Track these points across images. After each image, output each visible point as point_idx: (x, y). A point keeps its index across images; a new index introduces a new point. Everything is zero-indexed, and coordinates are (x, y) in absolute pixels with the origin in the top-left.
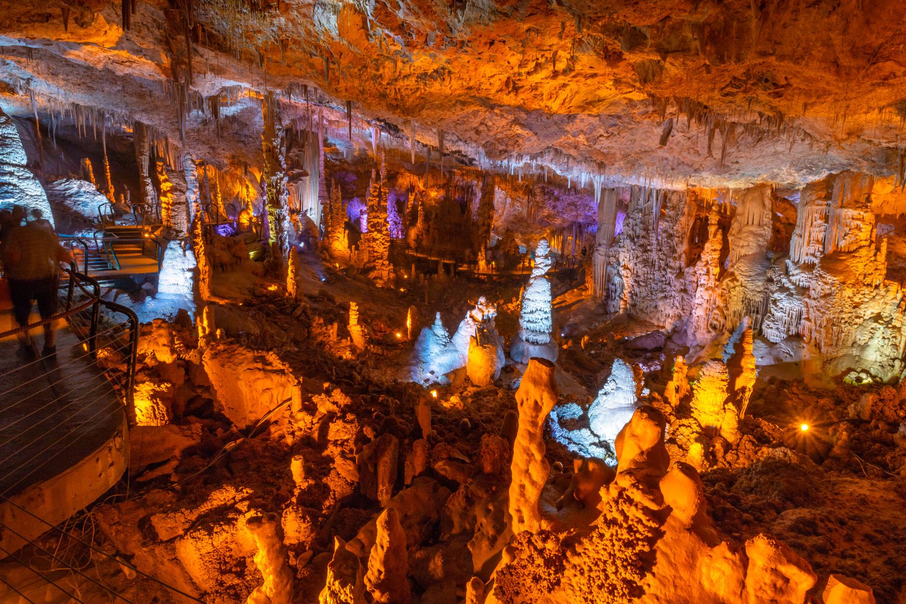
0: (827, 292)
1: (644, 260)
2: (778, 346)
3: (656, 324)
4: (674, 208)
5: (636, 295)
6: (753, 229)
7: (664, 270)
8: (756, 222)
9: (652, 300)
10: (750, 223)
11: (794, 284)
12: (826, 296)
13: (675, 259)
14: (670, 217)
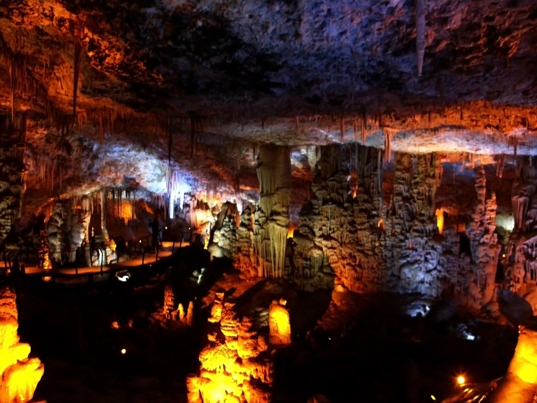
3: (401, 292)
4: (408, 170)
5: (360, 266)
7: (402, 234)
9: (387, 269)
13: (423, 222)
14: (404, 179)
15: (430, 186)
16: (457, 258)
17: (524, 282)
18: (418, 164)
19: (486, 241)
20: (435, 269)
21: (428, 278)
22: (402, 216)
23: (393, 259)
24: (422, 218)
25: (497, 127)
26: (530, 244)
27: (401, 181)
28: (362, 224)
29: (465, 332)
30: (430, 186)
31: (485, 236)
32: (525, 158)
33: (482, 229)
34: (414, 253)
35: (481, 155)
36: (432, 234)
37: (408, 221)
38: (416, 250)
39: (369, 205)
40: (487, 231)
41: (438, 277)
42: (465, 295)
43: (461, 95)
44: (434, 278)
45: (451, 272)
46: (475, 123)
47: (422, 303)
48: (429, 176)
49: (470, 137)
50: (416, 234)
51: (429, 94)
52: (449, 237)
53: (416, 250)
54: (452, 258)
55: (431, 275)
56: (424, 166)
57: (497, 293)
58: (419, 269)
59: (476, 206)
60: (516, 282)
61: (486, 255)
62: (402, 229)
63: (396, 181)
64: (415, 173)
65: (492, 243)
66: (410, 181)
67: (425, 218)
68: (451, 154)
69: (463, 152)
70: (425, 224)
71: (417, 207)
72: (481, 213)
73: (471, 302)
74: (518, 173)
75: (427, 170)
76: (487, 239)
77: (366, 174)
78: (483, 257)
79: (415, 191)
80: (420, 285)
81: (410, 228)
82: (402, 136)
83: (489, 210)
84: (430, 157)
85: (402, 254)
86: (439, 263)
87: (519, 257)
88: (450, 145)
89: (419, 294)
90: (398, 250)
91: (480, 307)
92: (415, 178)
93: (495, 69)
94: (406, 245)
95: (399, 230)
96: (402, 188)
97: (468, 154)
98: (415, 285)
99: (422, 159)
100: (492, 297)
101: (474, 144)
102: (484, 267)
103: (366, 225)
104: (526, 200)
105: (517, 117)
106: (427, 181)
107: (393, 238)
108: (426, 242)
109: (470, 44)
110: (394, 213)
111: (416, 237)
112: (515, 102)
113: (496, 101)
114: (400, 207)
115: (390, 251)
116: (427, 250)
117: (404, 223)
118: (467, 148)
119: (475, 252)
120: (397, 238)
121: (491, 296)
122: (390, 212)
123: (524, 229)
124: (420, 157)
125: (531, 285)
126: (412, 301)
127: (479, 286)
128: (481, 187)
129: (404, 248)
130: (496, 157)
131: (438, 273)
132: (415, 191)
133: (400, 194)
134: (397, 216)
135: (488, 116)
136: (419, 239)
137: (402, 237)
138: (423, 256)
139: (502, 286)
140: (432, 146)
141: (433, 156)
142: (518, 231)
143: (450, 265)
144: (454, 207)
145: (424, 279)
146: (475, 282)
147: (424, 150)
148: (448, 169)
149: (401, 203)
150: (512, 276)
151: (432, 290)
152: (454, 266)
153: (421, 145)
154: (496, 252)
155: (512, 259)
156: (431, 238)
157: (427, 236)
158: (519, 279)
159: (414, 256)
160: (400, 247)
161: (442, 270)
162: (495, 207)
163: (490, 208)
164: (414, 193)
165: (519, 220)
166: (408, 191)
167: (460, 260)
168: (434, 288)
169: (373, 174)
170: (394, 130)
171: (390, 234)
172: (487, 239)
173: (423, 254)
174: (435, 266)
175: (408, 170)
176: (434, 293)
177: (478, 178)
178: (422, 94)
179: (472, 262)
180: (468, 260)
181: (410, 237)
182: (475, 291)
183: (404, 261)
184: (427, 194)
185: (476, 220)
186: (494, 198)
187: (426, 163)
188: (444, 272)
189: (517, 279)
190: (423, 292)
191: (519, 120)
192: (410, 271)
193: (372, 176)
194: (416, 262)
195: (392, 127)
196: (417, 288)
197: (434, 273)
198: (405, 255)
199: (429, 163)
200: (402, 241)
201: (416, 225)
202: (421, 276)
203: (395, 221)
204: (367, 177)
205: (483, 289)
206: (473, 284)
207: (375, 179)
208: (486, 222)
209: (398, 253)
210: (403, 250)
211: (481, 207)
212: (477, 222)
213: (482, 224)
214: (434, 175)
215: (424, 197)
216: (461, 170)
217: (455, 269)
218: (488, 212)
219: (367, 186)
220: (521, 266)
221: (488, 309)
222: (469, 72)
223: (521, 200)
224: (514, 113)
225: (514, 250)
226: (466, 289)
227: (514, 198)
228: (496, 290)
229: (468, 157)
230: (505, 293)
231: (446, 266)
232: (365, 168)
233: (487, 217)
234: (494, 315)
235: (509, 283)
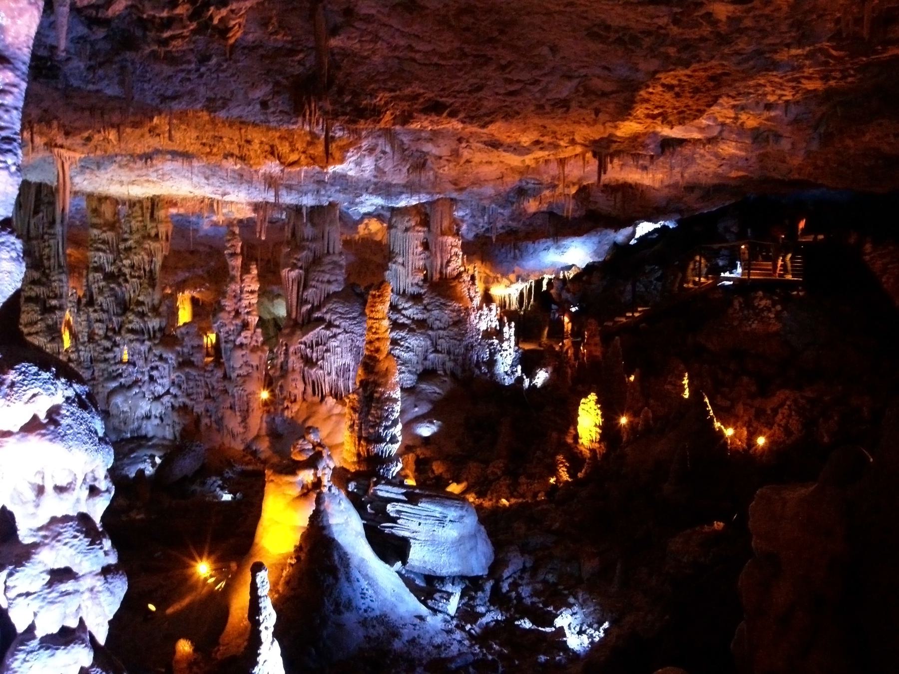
0: (456, 319)
1: (49, 327)
2: (418, 390)
4: (112, 226)
6: (335, 258)
7: (106, 337)
8: (336, 252)
10: (331, 251)
11: (409, 318)
12: (456, 323)
13: (142, 315)
14: (104, 242)
15: (151, 254)
16: (202, 373)
17: (304, 400)
18: (128, 216)
19: (245, 341)
20: (168, 392)
21: (157, 409)
22: (105, 306)
23: (95, 382)
24: (140, 309)
25: (242, 158)
26: (308, 342)
27: (100, 246)
28: (32, 323)
29: (218, 489)
30: (151, 254)
31: (243, 334)
32: (298, 209)
33: (238, 322)
34: (131, 369)
35: (232, 202)
36: (158, 335)
37: (117, 315)
38: (134, 365)
39: (42, 289)
40: (245, 326)
41: (173, 406)
42: (219, 430)
43: (164, 99)
44: (166, 408)
45: (194, 397)
46: (208, 150)
47: (149, 452)
48: (149, 237)
49: (208, 172)
50: (132, 337)
51: (109, 92)
52: (186, 339)
53: (134, 365)
54: (194, 372)
55: (162, 404)
56: (140, 219)
57: (266, 422)
58: (140, 395)
59: (227, 286)
60: (292, 402)
61: (246, 363)
62: (107, 329)
63: (91, 246)
64: (126, 232)
65: (254, 343)
66: (117, 246)
67: (145, 309)
68: (184, 199)
69: (204, 198)
70: (146, 319)
71: (130, 289)
72: (235, 297)
73: (227, 440)
74: (288, 233)
75: (146, 226)
76: (245, 337)
77: (33, 233)
78: (241, 367)
79: (127, 262)
80: (145, 422)
81: (120, 328)
82: (94, 167)
83: (248, 292)
84: (149, 204)
85: (110, 373)
86: (173, 383)
87: (295, 362)
88: (180, 184)
89: (145, 438)
90: (102, 366)
91: (242, 447)
92: (126, 240)
93: (214, 61)
94: (115, 357)
95: (101, 332)
96: (102, 258)
97: (212, 200)
98: (136, 424)
99: (137, 208)
100: (260, 429)
101: (218, 184)
102: (244, 382)
103: (40, 326)
104: (300, 274)
105: (261, 143)
106: (147, 246)
107: (91, 346)
108: (150, 349)
109: (163, 11)
110: (91, 302)
111: (131, 341)
112: (252, 119)
113: (222, 114)
114: (101, 291)
115: (88, 368)
116: (151, 362)
117: (110, 320)
118: (207, 191)
119: (229, 360)
120: (99, 345)
121: (258, 427)
122: (84, 301)
123: (300, 320)
124: (133, 203)
125: (313, 404)
126: (132, 451)
127: (238, 414)
128: (234, 255)
129: (112, 362)
130: (256, 207)
131: (172, 400)
132: (127, 262)
133: (99, 269)
134: (96, 307)
135: (221, 138)
136: (137, 345)
137: (108, 344)
138: (146, 373)
139: (272, 410)
140: (151, 185)
141: (154, 203)
142: (292, 323)
143: (191, 384)
144: (208, 289)
145: (150, 411)
146: (232, 408)
147: (139, 191)
148: (182, 226)
149: (102, 284)
150: (285, 393)
151: (165, 429)
152: (198, 386)
153: (133, 183)
154: (260, 358)
155: (285, 368)
156: (157, 342)
157: (150, 339)
158: (295, 396)
159: (130, 375)
160: (106, 360)
161: (179, 393)
162: (256, 286)
163: (249, 289)
164: (124, 266)
165: (291, 306)
166: (114, 263)
167: (206, 374)
168: (169, 425)
169: (46, 233)
170: (71, 154)
171: (86, 339)
172: (245, 337)
173: (146, 369)
174: (167, 389)
175: (112, 226)
176: (168, 433)
177: (229, 240)
178: (98, 91)
179: (226, 377)
180: (219, 374)
181: (122, 342)
182: (233, 422)
183: (114, 385)
184: (147, 269)
185: (227, 309)
186: (255, 272)
187: (143, 215)
188: (183, 397)
189: (293, 398)
190: (150, 435)
191: (267, 148)
192: (126, 401)
193: (46, 237)
194: (136, 383)
195: (69, 149)
196: (140, 427)
197: (166, 399)
198: (115, 374)
199: (148, 215)
200: (108, 350)
201: (130, 322)
202: (145, 407)
203: (94, 316)
204: (36, 238)
205: (244, 419)
206: (229, 412)
207: (52, 242)
208: (243, 311)
209: (104, 370)
210: (111, 365)
211: (235, 287)
212: (229, 312)
213: (237, 313)
214: (157, 235)
215: (142, 272)
216: (205, 226)
217: (199, 390)
218: (245, 295)
219: (37, 254)
220: (299, 377)
221: (254, 448)
222: (172, 59)
223: (294, 274)
224: (257, 137)
225: (286, 353)
226: (220, 421)
227: (284, 272)
228: (265, 416)
229: (212, 205)
230: (278, 420)
231: (184, 386)
232: (32, 222)
233: (245, 303)
234: (262, 456)
235: (283, 404)
